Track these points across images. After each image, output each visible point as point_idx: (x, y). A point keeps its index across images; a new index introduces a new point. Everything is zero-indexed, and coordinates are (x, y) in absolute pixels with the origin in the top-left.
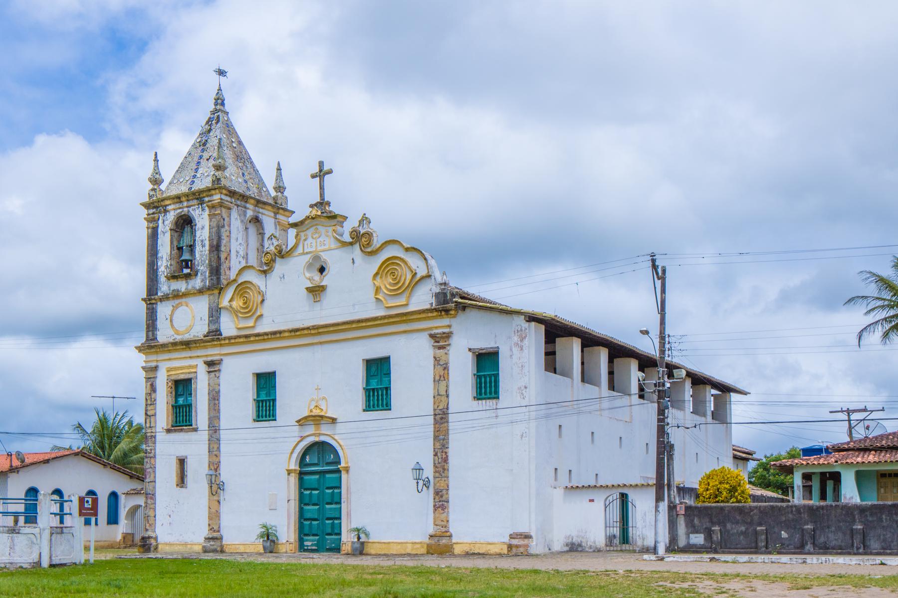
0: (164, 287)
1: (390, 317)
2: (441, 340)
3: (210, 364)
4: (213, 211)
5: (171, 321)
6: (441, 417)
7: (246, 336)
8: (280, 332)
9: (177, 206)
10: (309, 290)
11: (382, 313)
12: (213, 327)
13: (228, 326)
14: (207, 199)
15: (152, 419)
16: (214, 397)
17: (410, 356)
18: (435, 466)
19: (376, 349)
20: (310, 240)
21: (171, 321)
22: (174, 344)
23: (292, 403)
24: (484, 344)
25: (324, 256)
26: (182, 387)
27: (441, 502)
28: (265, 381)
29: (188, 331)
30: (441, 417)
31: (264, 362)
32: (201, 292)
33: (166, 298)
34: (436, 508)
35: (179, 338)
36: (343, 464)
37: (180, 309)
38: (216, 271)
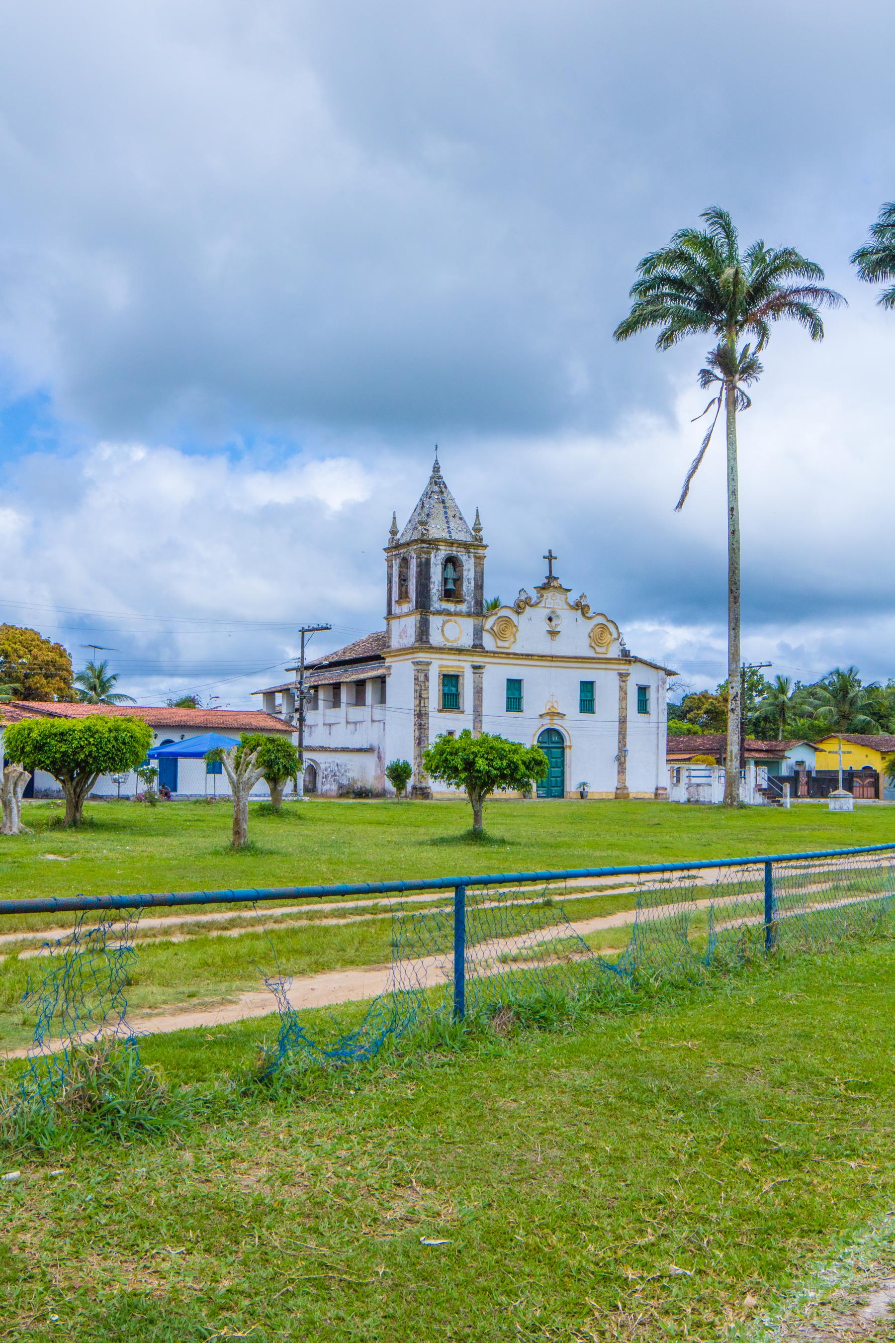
0: (436, 604)
1: (601, 659)
2: (623, 676)
3: (475, 667)
4: (478, 561)
5: (442, 631)
6: (623, 721)
7: (508, 654)
8: (532, 655)
9: (448, 548)
10: (549, 632)
11: (593, 655)
12: (477, 642)
13: (488, 642)
14: (472, 550)
15: (426, 701)
16: (478, 692)
17: (606, 683)
18: (619, 749)
19: (588, 676)
20: (549, 600)
21: (442, 631)
22: (451, 649)
23: (535, 701)
24: (644, 683)
25: (559, 612)
26: (451, 680)
27: (622, 770)
28: (514, 685)
29: (456, 640)
30: (623, 721)
31: (515, 672)
32: (469, 615)
33: (439, 613)
34: (619, 773)
35: (449, 645)
36: (568, 744)
37: (450, 623)
38: (479, 603)
